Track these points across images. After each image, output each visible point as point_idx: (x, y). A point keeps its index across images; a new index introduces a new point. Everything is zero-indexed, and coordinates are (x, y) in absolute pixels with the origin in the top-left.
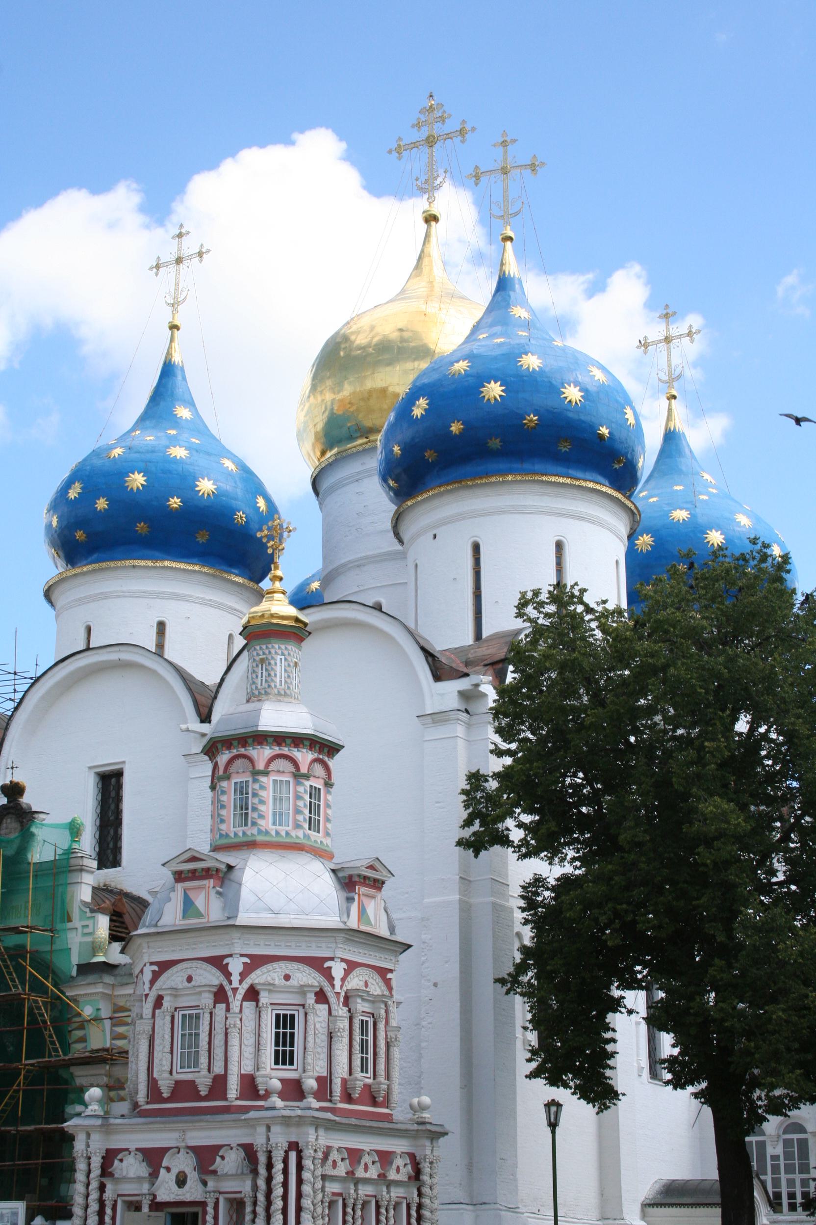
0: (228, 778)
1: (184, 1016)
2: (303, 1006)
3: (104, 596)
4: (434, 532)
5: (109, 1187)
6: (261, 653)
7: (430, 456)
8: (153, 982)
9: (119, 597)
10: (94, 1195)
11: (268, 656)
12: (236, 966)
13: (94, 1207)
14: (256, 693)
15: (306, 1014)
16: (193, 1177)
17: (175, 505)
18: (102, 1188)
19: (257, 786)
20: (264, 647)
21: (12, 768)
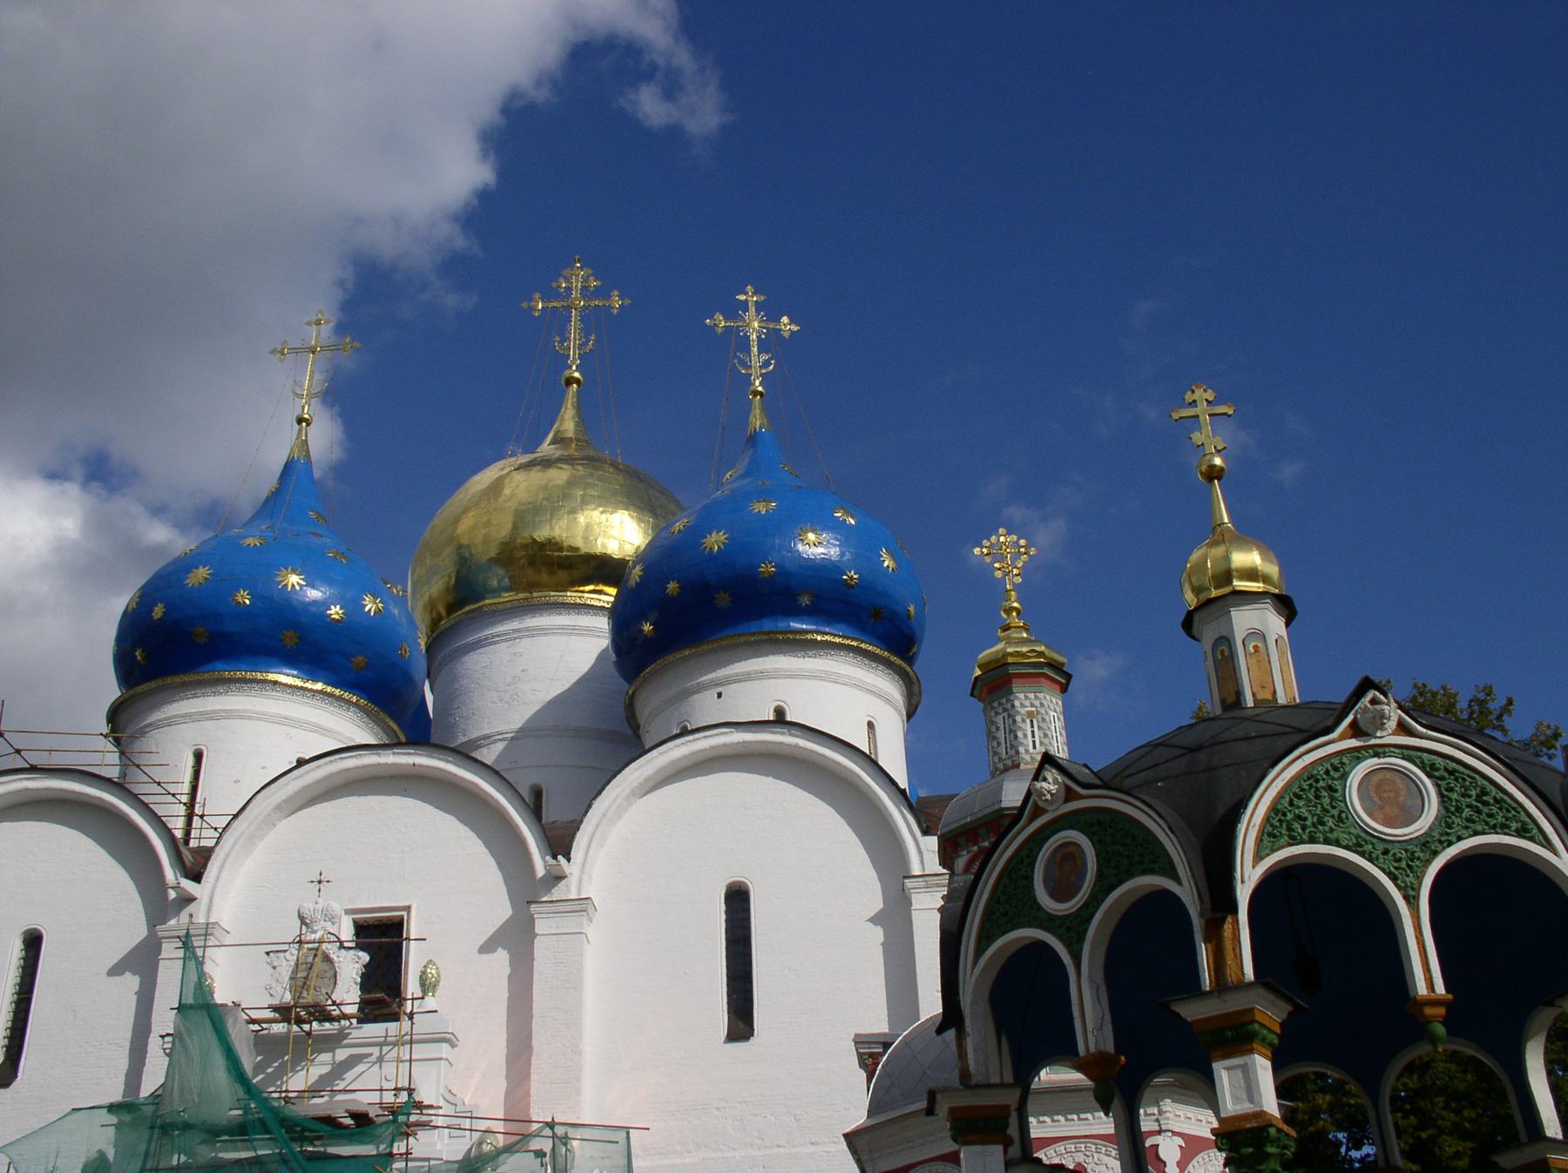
3: (229, 715)
4: (720, 689)
9: (250, 718)
11: (1039, 709)
14: (1001, 766)
17: (337, 617)
20: (1032, 696)
21: (320, 882)
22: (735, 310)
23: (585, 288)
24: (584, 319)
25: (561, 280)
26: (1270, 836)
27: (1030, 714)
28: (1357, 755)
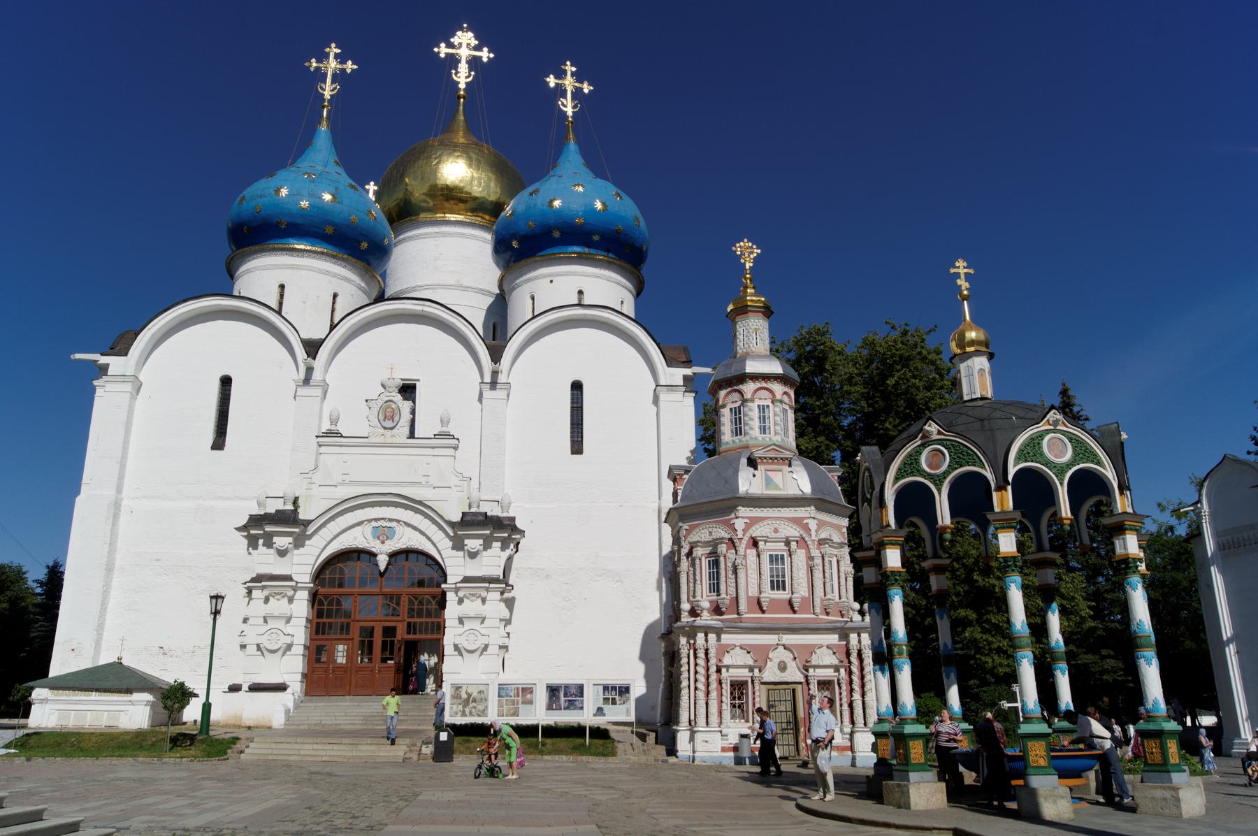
0: (752, 400)
1: (771, 556)
2: (836, 556)
4: (551, 279)
5: (724, 670)
6: (755, 324)
7: (557, 234)
8: (745, 531)
10: (714, 677)
12: (813, 525)
13: (714, 685)
15: (838, 561)
16: (792, 666)
18: (719, 671)
19: (777, 409)
20: (757, 321)
22: (561, 74)
23: (468, 45)
24: (468, 62)
25: (456, 37)
26: (1019, 459)
27: (756, 329)
28: (1048, 432)
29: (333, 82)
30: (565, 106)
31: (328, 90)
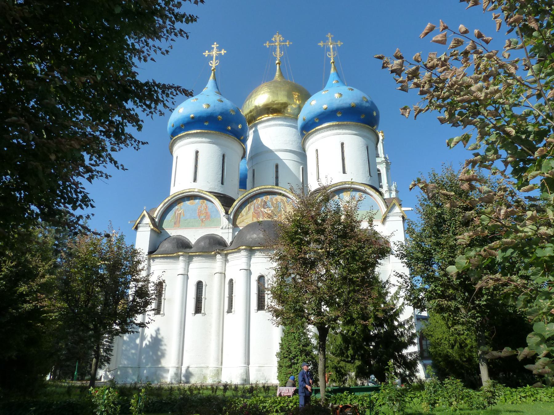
22: (325, 40)
29: (216, 59)
30: (330, 55)
31: (213, 64)
